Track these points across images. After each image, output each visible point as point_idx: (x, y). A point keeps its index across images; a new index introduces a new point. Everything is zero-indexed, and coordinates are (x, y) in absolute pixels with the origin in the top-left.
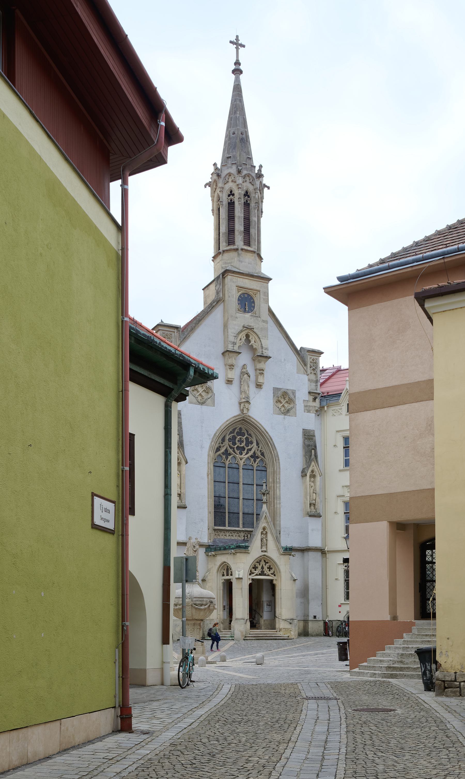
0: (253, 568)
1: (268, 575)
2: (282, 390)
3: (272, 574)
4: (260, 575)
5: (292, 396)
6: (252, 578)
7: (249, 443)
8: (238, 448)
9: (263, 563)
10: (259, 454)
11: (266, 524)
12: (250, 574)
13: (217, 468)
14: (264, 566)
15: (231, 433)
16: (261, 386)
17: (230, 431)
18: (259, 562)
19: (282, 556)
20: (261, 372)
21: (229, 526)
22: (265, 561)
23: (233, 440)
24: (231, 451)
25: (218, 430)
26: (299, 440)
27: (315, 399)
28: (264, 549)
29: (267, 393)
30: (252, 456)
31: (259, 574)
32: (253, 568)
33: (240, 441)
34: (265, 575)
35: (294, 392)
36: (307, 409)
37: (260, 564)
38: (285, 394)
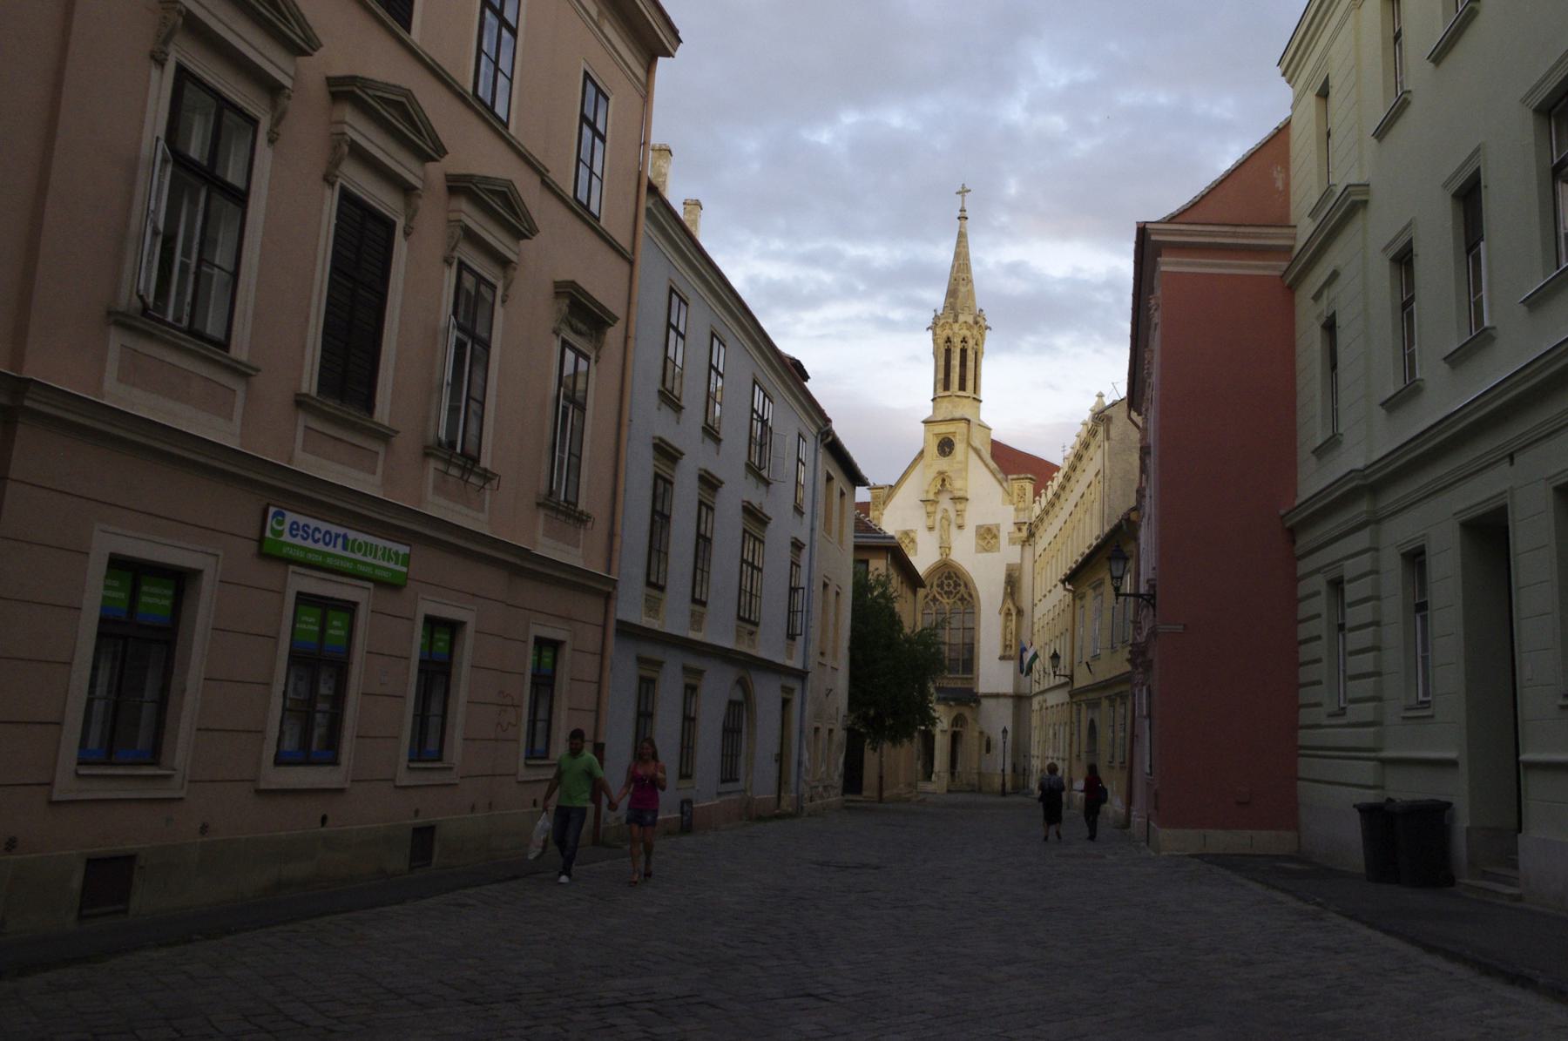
5: (995, 531)
7: (957, 585)
8: (946, 592)
10: (966, 596)
15: (939, 578)
17: (937, 577)
20: (959, 513)
24: (937, 596)
26: (1002, 577)
27: (1020, 530)
29: (970, 531)
30: (959, 600)
33: (949, 585)
35: (998, 526)
38: (989, 530)
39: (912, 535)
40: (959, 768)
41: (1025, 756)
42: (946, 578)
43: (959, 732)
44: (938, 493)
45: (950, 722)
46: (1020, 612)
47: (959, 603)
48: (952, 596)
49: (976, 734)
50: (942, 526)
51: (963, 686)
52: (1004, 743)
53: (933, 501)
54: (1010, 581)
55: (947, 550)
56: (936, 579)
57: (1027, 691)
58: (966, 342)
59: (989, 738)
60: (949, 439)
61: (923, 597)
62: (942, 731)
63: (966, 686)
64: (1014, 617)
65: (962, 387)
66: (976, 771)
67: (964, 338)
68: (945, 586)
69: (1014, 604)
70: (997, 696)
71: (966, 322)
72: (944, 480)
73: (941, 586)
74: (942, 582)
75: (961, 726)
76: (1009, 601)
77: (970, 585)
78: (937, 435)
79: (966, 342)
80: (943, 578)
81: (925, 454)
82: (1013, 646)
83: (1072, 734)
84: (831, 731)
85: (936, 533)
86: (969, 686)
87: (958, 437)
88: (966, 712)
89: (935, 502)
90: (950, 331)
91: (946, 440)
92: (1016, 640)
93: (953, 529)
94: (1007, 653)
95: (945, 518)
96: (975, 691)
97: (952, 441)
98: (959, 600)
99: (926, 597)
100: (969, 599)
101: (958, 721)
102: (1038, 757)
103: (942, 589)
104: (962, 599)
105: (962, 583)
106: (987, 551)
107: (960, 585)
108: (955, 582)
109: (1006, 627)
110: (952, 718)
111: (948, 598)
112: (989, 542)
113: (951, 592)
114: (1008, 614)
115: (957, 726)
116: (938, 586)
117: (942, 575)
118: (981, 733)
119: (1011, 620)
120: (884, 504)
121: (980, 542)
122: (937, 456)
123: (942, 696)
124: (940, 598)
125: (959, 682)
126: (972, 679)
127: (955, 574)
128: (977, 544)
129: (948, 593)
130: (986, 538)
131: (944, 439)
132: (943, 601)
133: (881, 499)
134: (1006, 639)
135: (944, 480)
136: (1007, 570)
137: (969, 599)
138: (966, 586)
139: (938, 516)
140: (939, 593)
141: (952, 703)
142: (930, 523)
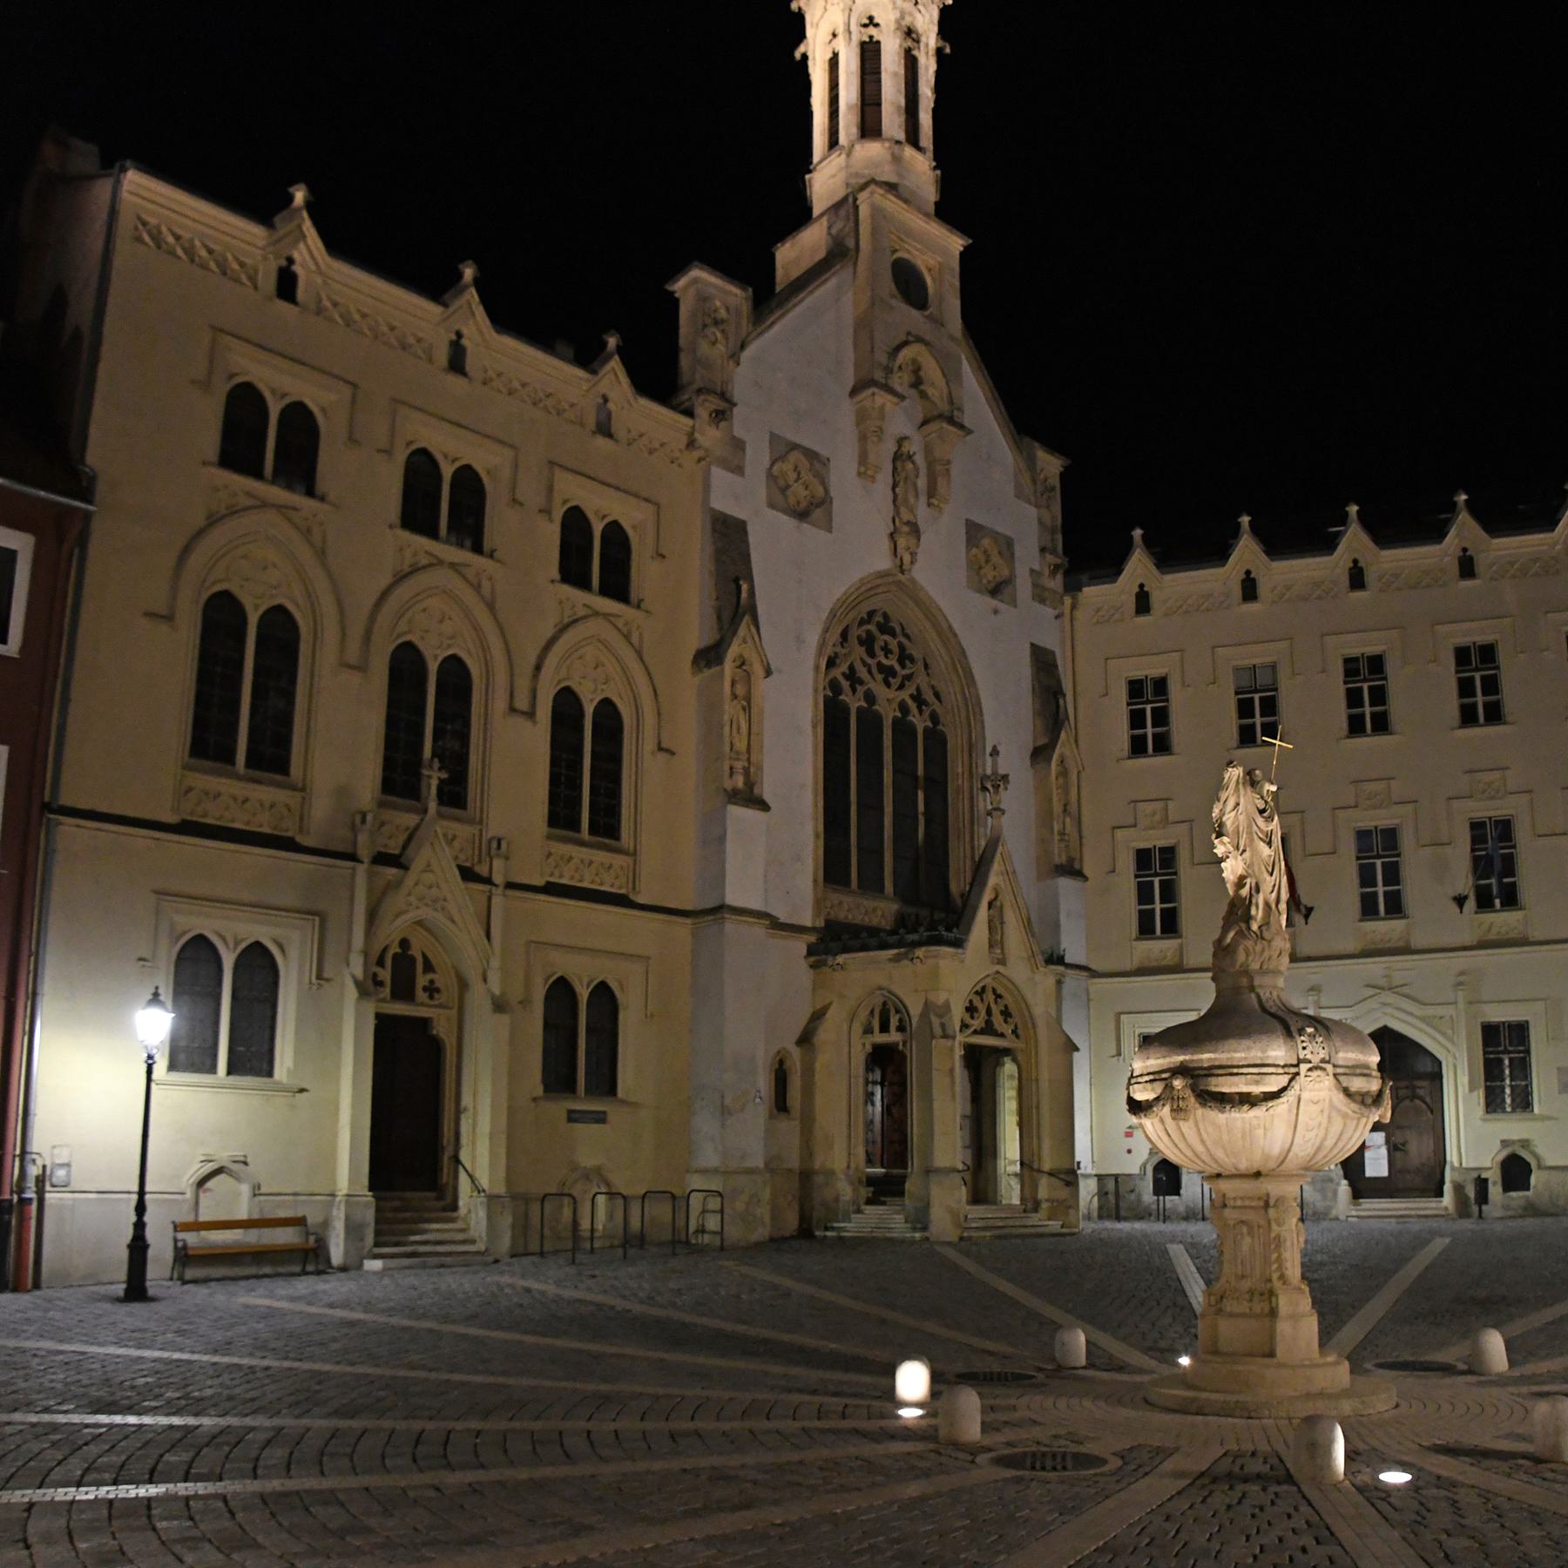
1: (1002, 1035)
6: (967, 1040)
10: (928, 696)
11: (1001, 877)
14: (993, 1006)
18: (981, 993)
24: (862, 673)
31: (982, 1029)
33: (887, 651)
36: (1040, 595)
37: (982, 1000)
104: (918, 698)
140: (864, 663)
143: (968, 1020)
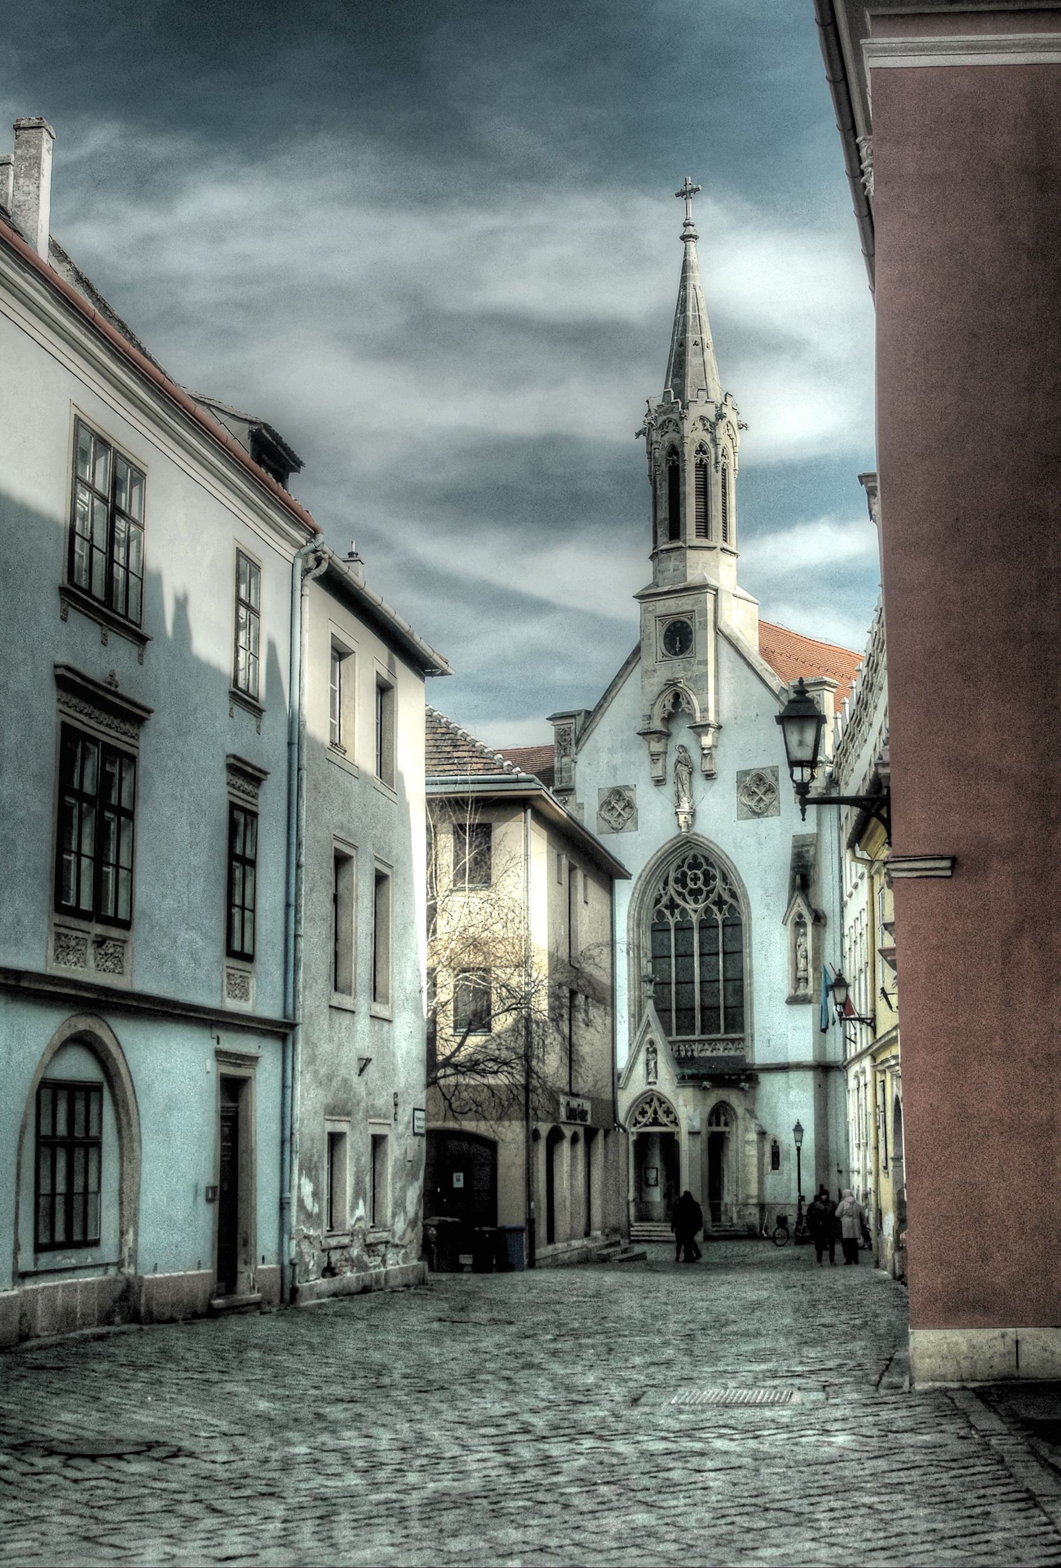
0: (640, 1113)
1: (665, 1125)
2: (753, 773)
3: (672, 1122)
4: (651, 1124)
5: (770, 779)
7: (708, 878)
8: (692, 892)
9: (655, 1103)
10: (726, 896)
12: (635, 1125)
13: (658, 933)
16: (713, 775)
17: (675, 864)
19: (679, 1090)
21: (677, 1034)
22: (659, 1100)
23: (681, 881)
25: (643, 871)
28: (651, 1080)
32: (640, 1113)
33: (695, 879)
34: (660, 1125)
38: (760, 779)
39: (627, 794)
40: (727, 1198)
41: (840, 1172)
42: (691, 868)
43: (723, 1133)
44: (668, 719)
45: (706, 1116)
46: (819, 918)
47: (715, 908)
48: (701, 898)
49: (753, 1136)
50: (678, 776)
51: (726, 1053)
52: (799, 1149)
53: (660, 732)
54: (798, 866)
55: (689, 817)
56: (672, 868)
57: (840, 1057)
58: (705, 453)
59: (775, 1142)
60: (683, 623)
61: (653, 901)
62: (690, 1133)
63: (732, 1053)
64: (810, 929)
65: (704, 530)
66: (754, 1201)
67: (701, 446)
68: (689, 881)
69: (809, 906)
70: (784, 1068)
71: (702, 418)
72: (677, 696)
73: (681, 881)
74: (684, 874)
75: (726, 1124)
76: (799, 901)
77: (732, 877)
78: (661, 617)
79: (705, 453)
80: (685, 869)
81: (643, 653)
82: (811, 979)
83: (878, 1128)
84: (378, 1141)
85: (669, 789)
86: (738, 1053)
87: (697, 619)
88: (734, 1099)
89: (665, 735)
90: (675, 435)
91: (679, 625)
92: (815, 969)
93: (699, 780)
94: (801, 992)
95: (684, 762)
96: (748, 1060)
97: (688, 626)
98: (715, 903)
99: (658, 901)
100: (730, 900)
101: (719, 1114)
102: (859, 1172)
103: (684, 885)
104: (720, 903)
105: (718, 875)
106: (758, 815)
107: (714, 878)
108: (706, 873)
109: (796, 947)
110: (708, 1109)
111: (696, 901)
112: (761, 800)
113: (699, 891)
114: (799, 924)
115: (718, 1124)
116: (677, 881)
117: (683, 861)
118: (762, 1134)
119: (805, 934)
120: (577, 743)
121: (745, 800)
122: (664, 655)
123: (688, 1072)
124: (682, 903)
125: (721, 1046)
126: (742, 1040)
127: (706, 859)
128: (741, 804)
129: (695, 893)
130: (754, 792)
131: (674, 624)
132: (687, 906)
133: (572, 735)
134: (797, 968)
135: (677, 696)
136: (794, 847)
137: (730, 900)
138: (725, 878)
139: (672, 759)
140: (679, 894)
141: (706, 1084)
142: (658, 772)
143: (640, 1119)
